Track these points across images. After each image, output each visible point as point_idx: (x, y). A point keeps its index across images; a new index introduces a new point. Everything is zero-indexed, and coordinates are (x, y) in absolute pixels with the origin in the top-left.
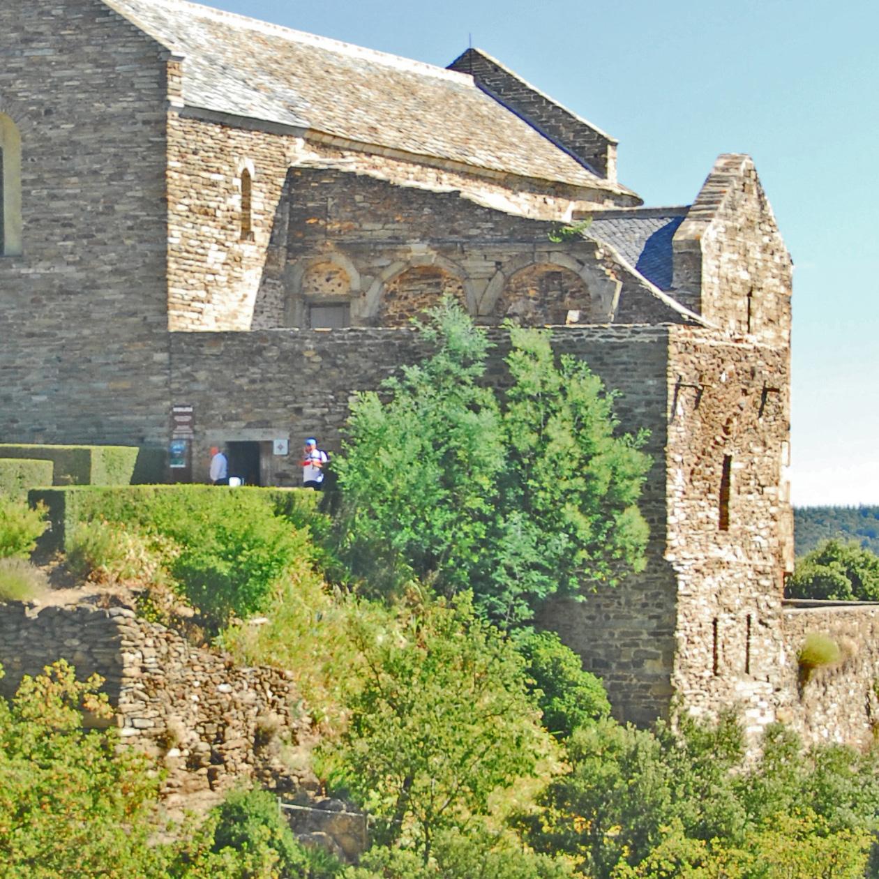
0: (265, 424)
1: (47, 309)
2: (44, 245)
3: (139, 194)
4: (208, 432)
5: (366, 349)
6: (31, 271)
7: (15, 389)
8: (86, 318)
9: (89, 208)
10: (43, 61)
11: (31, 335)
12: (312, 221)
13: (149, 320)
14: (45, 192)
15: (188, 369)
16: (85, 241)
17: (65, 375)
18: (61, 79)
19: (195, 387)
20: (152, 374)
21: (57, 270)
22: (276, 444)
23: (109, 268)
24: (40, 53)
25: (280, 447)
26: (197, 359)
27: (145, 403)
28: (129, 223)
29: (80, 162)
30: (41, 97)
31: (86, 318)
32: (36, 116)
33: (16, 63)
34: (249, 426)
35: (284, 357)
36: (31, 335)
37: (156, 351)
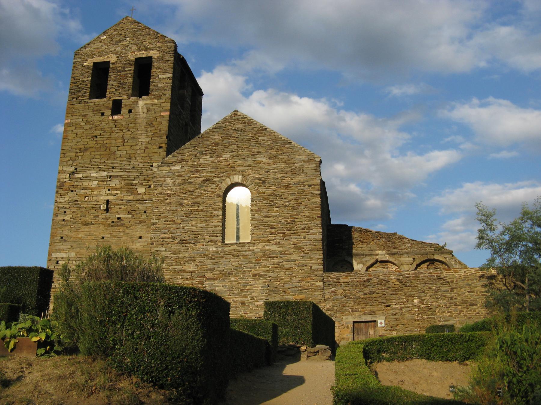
0: (372, 313)
1: (263, 264)
2: (262, 236)
3: (307, 214)
4: (344, 317)
5: (421, 278)
6: (255, 247)
7: (247, 299)
8: (283, 268)
9: (283, 221)
10: (261, 162)
11: (255, 275)
12: (337, 245)
14: (262, 214)
15: (333, 289)
16: (281, 235)
17: (272, 293)
19: (337, 297)
20: (315, 292)
21: (268, 247)
22: (379, 322)
23: (293, 246)
24: (260, 159)
25: (381, 323)
28: (303, 226)
29: (279, 202)
30: (260, 176)
31: (283, 268)
32: (258, 184)
33: (248, 163)
34: (364, 314)
35: (380, 283)
36: (255, 275)
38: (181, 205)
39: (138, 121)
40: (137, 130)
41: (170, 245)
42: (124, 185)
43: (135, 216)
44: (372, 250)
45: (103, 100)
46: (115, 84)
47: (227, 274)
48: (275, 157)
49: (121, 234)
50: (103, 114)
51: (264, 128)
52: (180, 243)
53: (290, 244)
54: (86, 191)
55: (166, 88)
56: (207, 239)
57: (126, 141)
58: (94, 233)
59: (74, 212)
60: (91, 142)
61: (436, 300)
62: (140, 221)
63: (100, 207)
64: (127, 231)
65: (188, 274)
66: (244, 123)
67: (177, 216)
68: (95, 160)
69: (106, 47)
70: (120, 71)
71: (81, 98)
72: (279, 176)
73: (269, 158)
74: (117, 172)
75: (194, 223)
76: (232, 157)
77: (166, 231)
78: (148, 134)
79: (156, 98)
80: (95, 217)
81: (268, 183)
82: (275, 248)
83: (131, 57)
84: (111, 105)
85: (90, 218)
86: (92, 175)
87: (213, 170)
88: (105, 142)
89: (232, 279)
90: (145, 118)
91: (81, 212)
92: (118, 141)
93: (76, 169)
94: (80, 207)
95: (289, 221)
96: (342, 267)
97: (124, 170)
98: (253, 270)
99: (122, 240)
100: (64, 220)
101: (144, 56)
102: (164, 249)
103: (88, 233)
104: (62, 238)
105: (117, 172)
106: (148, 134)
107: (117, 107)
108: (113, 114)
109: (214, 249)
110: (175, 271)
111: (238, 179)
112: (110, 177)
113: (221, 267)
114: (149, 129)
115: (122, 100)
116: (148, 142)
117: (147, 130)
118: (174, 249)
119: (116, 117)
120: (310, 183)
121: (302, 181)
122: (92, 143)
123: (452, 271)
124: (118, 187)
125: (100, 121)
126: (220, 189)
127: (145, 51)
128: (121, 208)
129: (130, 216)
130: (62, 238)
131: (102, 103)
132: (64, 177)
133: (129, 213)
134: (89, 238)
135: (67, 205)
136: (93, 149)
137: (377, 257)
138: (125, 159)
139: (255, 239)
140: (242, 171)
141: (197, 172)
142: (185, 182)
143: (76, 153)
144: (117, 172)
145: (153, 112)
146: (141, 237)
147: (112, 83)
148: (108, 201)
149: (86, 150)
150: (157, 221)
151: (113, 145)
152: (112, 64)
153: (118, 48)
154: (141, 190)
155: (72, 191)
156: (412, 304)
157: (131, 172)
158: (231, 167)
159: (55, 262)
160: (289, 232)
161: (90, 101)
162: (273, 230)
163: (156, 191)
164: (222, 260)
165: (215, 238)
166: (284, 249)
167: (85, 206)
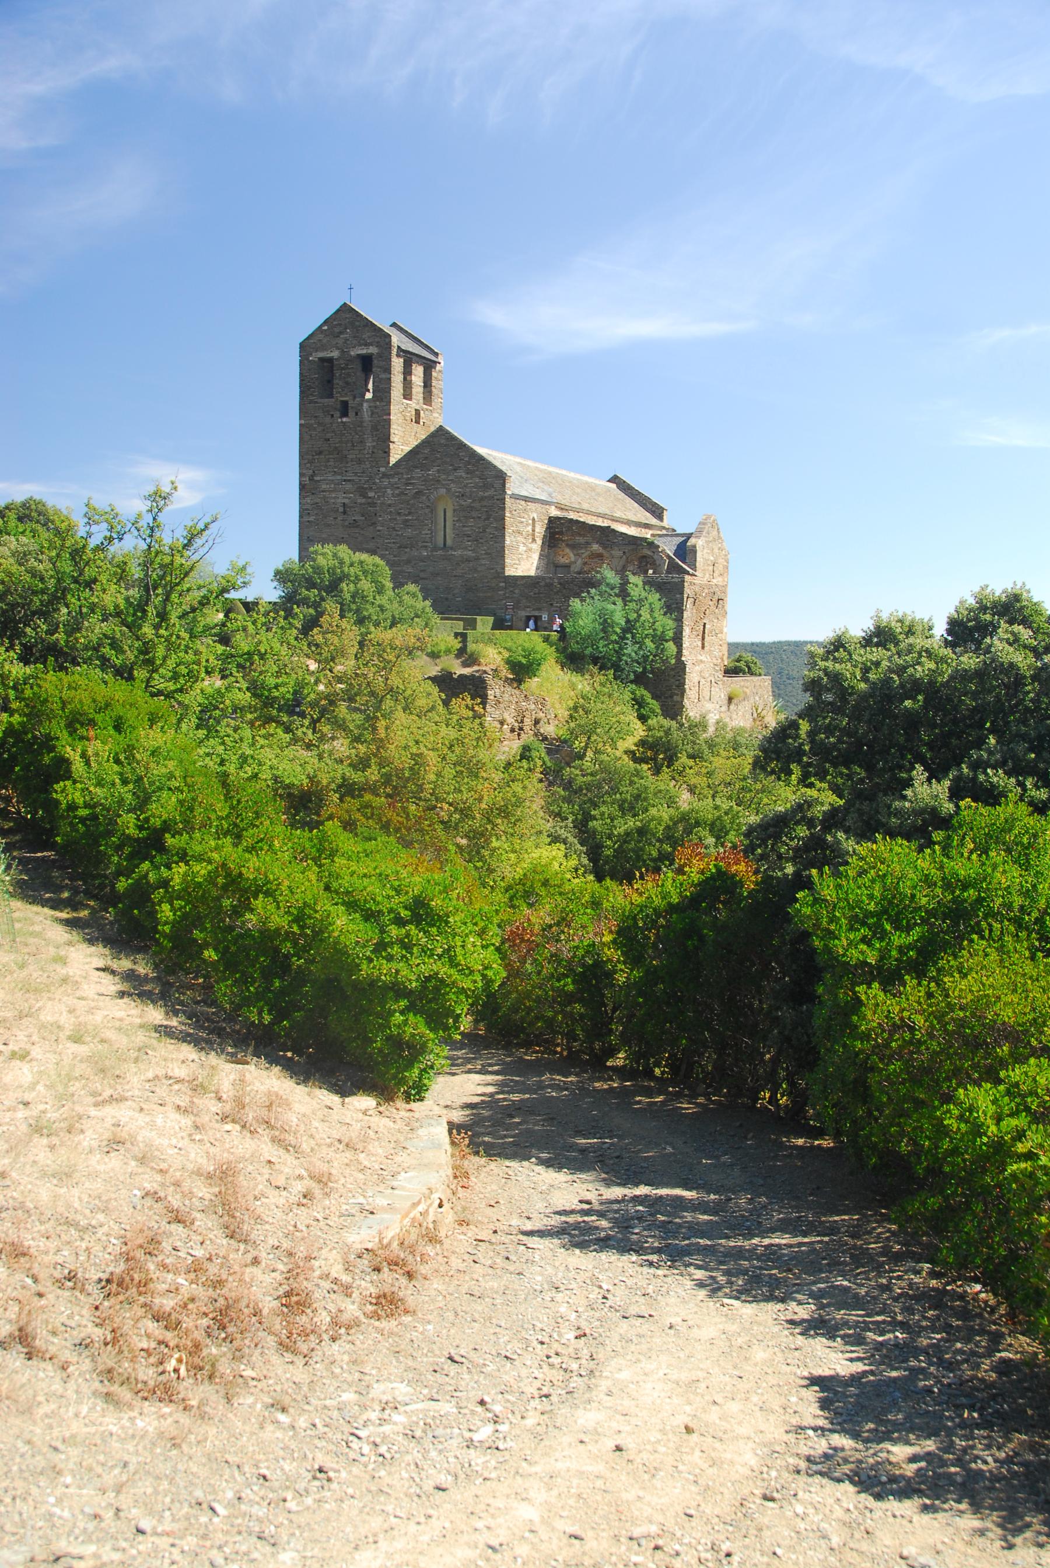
0: (539, 609)
10: (461, 477)
29: (474, 514)
32: (458, 497)
35: (547, 585)
38: (399, 514)
39: (365, 424)
50: (332, 416)
52: (399, 547)
56: (420, 544)
70: (343, 369)
76: (438, 471)
84: (339, 406)
85: (330, 520)
94: (321, 509)
101: (364, 352)
108: (341, 417)
116: (374, 447)
119: (344, 420)
142: (402, 493)
149: (320, 453)
154: (371, 494)
161: (319, 400)
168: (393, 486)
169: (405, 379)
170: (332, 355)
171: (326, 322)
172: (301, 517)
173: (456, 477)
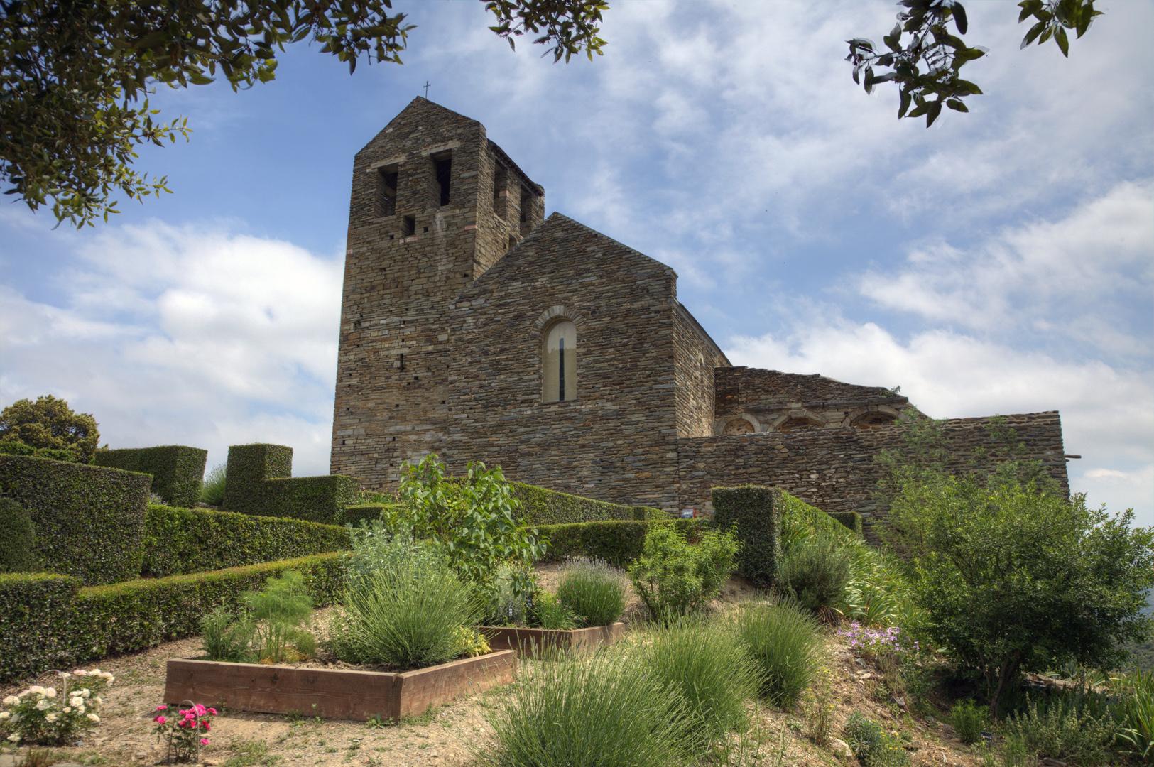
3: (654, 354)
5: (821, 442)
6: (583, 407)
7: (573, 481)
9: (621, 366)
10: (591, 284)
11: (583, 446)
12: (730, 397)
13: (663, 432)
14: (592, 359)
16: (618, 387)
18: (602, 293)
19: (697, 473)
20: (665, 467)
23: (635, 401)
26: (697, 455)
27: (662, 486)
31: (619, 433)
37: (668, 451)
38: (486, 353)
39: (437, 242)
40: (436, 255)
41: (473, 411)
42: (422, 331)
43: (436, 373)
44: (781, 403)
45: (391, 217)
46: (406, 193)
47: (545, 446)
48: (609, 274)
49: (420, 399)
50: (392, 237)
51: (593, 233)
52: (484, 407)
53: (630, 400)
54: (375, 344)
55: (470, 191)
56: (520, 398)
57: (422, 270)
58: (387, 401)
59: (361, 374)
60: (377, 278)
61: (843, 474)
62: (443, 380)
63: (392, 365)
64: (427, 395)
65: (497, 449)
66: (566, 230)
67: (481, 369)
68: (384, 301)
69: (393, 144)
70: (411, 175)
71: (364, 218)
72: (614, 301)
73: (601, 277)
74: (412, 316)
75: (502, 377)
77: (468, 391)
78: (449, 259)
79: (457, 207)
80: (387, 378)
81: (600, 313)
82: (611, 407)
83: (424, 154)
85: (381, 382)
86: (382, 322)
87: (527, 301)
88: (396, 275)
89: (553, 452)
90: (445, 236)
91: (370, 373)
92: (412, 273)
93: (361, 316)
95: (628, 365)
96: (738, 430)
97: (420, 311)
98: (580, 439)
99: (420, 407)
100: (349, 386)
101: (442, 149)
102: (464, 416)
103: (379, 401)
104: (348, 409)
105: (412, 316)
106: (449, 259)
107: (410, 225)
109: (529, 412)
110: (479, 446)
111: (558, 310)
112: (404, 322)
113: (538, 437)
114: (451, 251)
115: (414, 215)
116: (449, 271)
117: (448, 254)
118: (477, 416)
119: (408, 240)
120: (657, 308)
121: (647, 305)
122: (380, 279)
123: (870, 429)
124: (413, 336)
125: (389, 247)
126: (536, 326)
127: (442, 142)
128: (418, 364)
129: (430, 374)
130: (348, 409)
131: (390, 222)
132: (348, 328)
133: (429, 369)
134: (381, 407)
135: (353, 366)
136: (382, 287)
137: (789, 412)
138: (421, 296)
139: (583, 395)
140: (565, 298)
141: (505, 305)
143: (362, 294)
144: (412, 315)
145: (455, 228)
146: (444, 402)
147: (402, 192)
148: (402, 355)
149: (373, 288)
150: (456, 378)
151: (406, 278)
152: (401, 166)
153: (409, 143)
154: (442, 337)
155: (358, 346)
156: (808, 482)
157: (430, 314)
158: (550, 295)
159: (341, 442)
160: (628, 382)
161: (375, 220)
162: (607, 380)
163: (454, 337)
164: (540, 428)
165: (530, 397)
166: (622, 406)
167: (375, 364)
168: (477, 312)
169: (496, 196)
170: (397, 160)
171: (390, 125)
172: (339, 380)
173: (583, 285)
